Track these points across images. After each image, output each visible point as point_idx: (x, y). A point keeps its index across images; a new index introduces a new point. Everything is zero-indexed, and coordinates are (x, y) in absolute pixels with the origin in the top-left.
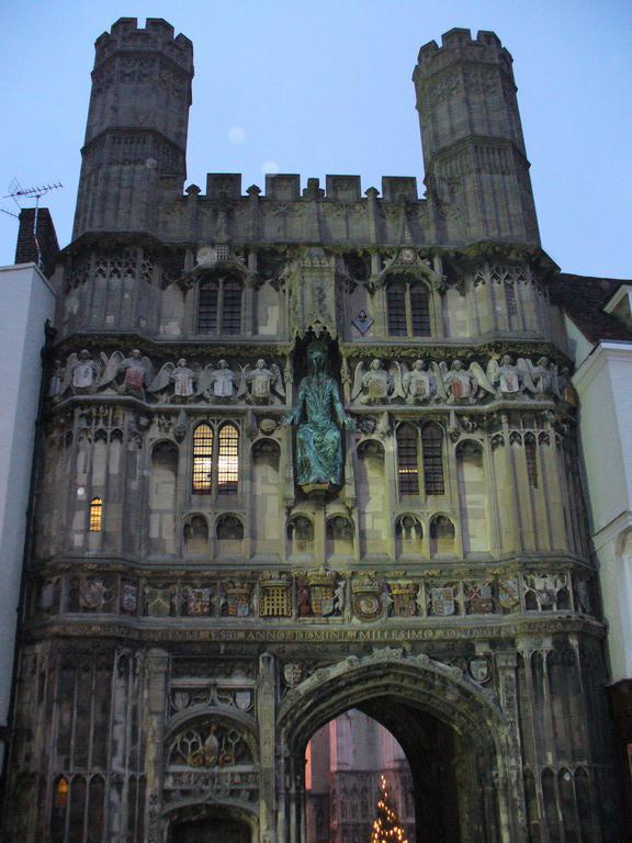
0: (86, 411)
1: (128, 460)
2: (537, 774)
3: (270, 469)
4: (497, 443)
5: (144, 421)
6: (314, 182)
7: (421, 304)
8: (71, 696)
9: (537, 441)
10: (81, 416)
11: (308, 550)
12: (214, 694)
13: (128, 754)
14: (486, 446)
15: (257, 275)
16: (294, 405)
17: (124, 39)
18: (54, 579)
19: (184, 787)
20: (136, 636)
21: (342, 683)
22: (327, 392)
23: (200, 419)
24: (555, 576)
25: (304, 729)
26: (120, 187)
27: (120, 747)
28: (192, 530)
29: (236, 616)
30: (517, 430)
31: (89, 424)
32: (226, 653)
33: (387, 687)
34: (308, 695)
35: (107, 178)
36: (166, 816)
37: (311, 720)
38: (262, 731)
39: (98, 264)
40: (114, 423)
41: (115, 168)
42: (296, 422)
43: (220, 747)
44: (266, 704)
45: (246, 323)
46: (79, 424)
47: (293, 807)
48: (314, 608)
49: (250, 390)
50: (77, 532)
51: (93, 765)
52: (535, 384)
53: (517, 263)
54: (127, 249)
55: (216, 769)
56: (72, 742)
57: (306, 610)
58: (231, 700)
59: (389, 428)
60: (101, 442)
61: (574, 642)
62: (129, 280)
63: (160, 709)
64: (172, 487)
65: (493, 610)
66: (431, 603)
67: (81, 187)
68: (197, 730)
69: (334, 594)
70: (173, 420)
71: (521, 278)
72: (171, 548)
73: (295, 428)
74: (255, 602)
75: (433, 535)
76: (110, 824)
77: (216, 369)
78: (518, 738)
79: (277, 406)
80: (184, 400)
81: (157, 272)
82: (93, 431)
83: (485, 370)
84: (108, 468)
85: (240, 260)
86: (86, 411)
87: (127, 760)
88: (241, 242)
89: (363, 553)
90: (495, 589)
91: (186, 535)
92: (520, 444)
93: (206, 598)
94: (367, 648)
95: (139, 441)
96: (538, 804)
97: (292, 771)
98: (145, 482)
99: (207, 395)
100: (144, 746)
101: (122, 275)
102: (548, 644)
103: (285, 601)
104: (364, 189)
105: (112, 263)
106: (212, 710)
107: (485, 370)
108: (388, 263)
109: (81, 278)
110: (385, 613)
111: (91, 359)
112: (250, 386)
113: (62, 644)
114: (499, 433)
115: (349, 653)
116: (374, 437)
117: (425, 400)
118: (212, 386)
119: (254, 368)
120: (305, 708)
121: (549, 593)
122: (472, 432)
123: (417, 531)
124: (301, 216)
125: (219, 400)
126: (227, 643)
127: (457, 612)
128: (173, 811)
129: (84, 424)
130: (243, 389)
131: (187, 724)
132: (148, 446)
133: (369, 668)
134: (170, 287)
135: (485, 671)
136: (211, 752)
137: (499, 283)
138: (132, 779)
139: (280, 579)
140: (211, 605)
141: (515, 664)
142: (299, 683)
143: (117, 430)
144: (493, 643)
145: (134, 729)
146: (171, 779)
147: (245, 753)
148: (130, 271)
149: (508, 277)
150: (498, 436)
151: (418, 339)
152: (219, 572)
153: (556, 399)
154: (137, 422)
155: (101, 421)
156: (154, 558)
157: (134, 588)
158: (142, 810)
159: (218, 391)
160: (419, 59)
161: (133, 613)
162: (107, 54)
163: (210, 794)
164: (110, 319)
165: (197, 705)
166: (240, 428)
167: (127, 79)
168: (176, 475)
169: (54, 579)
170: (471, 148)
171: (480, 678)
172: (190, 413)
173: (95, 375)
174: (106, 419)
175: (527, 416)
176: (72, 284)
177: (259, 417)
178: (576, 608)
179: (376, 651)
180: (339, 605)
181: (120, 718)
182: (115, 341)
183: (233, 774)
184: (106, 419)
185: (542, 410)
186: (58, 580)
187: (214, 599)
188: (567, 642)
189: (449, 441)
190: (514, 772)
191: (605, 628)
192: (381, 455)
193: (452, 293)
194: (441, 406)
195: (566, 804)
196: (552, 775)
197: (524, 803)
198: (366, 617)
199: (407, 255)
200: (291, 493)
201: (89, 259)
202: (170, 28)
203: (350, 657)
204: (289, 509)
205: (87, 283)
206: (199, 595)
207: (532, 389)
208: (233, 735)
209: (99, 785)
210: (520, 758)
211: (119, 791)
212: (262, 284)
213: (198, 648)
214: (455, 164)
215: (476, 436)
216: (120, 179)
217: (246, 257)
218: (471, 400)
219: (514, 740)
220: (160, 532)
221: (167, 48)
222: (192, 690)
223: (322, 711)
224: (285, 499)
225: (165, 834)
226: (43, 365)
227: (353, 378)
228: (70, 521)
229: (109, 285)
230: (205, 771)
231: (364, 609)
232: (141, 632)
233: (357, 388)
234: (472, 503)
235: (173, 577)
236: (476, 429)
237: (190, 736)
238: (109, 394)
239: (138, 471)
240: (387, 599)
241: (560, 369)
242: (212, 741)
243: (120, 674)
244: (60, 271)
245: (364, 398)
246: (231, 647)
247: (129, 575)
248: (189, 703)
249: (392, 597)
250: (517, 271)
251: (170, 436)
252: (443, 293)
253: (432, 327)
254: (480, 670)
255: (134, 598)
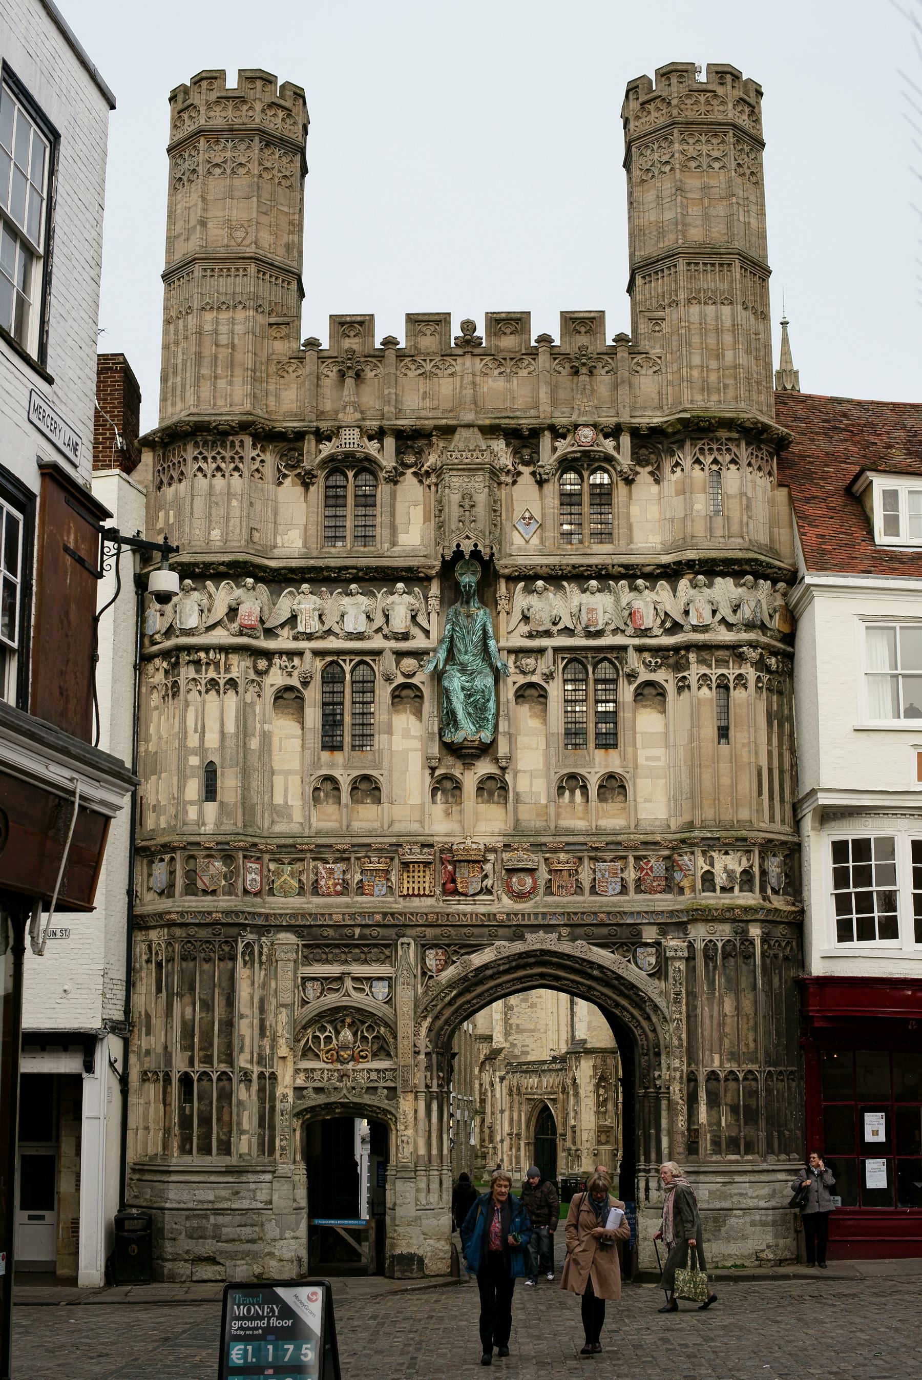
0: (194, 657)
1: (244, 713)
2: (702, 1078)
3: (412, 718)
4: (683, 686)
5: (262, 664)
6: (469, 326)
7: (603, 496)
8: (192, 989)
9: (731, 685)
10: (189, 662)
11: (456, 816)
12: (349, 983)
13: (256, 1049)
14: (671, 688)
15: (395, 468)
16: (441, 642)
17: (209, 106)
18: (167, 857)
19: (318, 1084)
20: (260, 921)
21: (489, 972)
22: (478, 626)
23: (329, 659)
24: (739, 854)
25: (446, 1022)
26: (217, 345)
27: (247, 1042)
28: (322, 794)
29: (372, 895)
30: (708, 671)
31: (198, 671)
32: (362, 937)
33: (542, 976)
34: (451, 985)
35: (199, 333)
36: (298, 1115)
37: (456, 1011)
38: (400, 1024)
39: (196, 458)
40: (227, 670)
41: (208, 316)
42: (441, 666)
43: (355, 1042)
44: (405, 997)
45: (381, 532)
46: (187, 673)
47: (435, 1106)
48: (459, 886)
49: (387, 622)
50: (191, 803)
51: (220, 1062)
52: (735, 611)
53: (728, 439)
54: (231, 438)
55: (350, 1066)
56: (196, 1040)
57: (451, 889)
58: (367, 989)
59: (552, 668)
60: (213, 692)
61: (755, 931)
62: (236, 481)
63: (288, 1001)
64: (297, 742)
65: (668, 889)
66: (594, 879)
67: (166, 332)
68: (330, 1022)
69: (482, 869)
70: (296, 661)
71: (733, 461)
72: (297, 816)
73: (438, 676)
74: (393, 879)
75: (602, 797)
76: (239, 1123)
77: (348, 595)
78: (684, 1036)
79: (419, 642)
80: (310, 637)
81: (269, 470)
82: (203, 682)
83: (674, 590)
84: (222, 725)
85: (372, 448)
86: (194, 657)
87: (255, 1055)
88: (373, 424)
89: (517, 821)
90: (671, 864)
91: (316, 800)
92: (710, 688)
93: (338, 875)
94: (517, 932)
95: (257, 689)
96: (703, 1109)
97: (435, 1068)
98: (266, 737)
99: (336, 629)
100: (274, 1040)
101: (227, 475)
102: (724, 931)
103: (427, 878)
104: (534, 336)
105: (214, 458)
106: (346, 1001)
107: (674, 590)
108: (563, 446)
109: (175, 475)
110: (541, 890)
111: (195, 589)
112: (387, 617)
113: (178, 932)
114: (685, 674)
115: (496, 937)
116: (535, 679)
117: (598, 631)
118: (343, 616)
119: (392, 594)
120: (448, 998)
121: (730, 874)
122: (655, 671)
123: (582, 794)
124: (451, 375)
125: (350, 636)
126: (360, 925)
127: (624, 890)
128: (305, 1109)
129: (192, 674)
130: (379, 621)
131: (320, 1016)
132: (269, 694)
133: (521, 955)
134: (288, 482)
135: (653, 960)
136: (345, 1047)
137: (702, 469)
138: (261, 1076)
139: (421, 854)
140: (345, 883)
141: (686, 955)
142: (441, 970)
143: (231, 679)
144: (664, 928)
145: (262, 1022)
146: (302, 1075)
147: (383, 1050)
148: (236, 469)
149: (715, 461)
150: (684, 677)
151: (597, 548)
152: (353, 846)
153: (763, 627)
154: (255, 667)
155: (212, 667)
156: (279, 828)
157: (258, 866)
158: (273, 1109)
159: (350, 627)
160: (627, 96)
161: (257, 894)
162: (189, 127)
163: (345, 1091)
164: (216, 534)
165: (329, 996)
166: (376, 668)
167: (218, 171)
168: (303, 729)
169: (167, 857)
170: (681, 265)
171: (646, 967)
172: (317, 653)
173: (202, 611)
174: (217, 665)
175: (720, 653)
176: (165, 481)
177: (400, 655)
178: (763, 890)
179: (528, 936)
180: (489, 882)
181: (245, 1010)
182: (222, 568)
183: (370, 1070)
184: (217, 665)
185: (741, 646)
186: (172, 859)
187: (349, 877)
188: (745, 932)
189: (626, 682)
190: (678, 1074)
191: (802, 912)
192: (542, 700)
193: (644, 473)
194: (619, 640)
195: (734, 1109)
196: (717, 1079)
197: (685, 1108)
198: (520, 896)
199: (586, 435)
200: (435, 750)
201: (185, 450)
202: (268, 79)
203: (497, 943)
204: (433, 769)
205: (183, 484)
206: (331, 872)
207: (731, 619)
208: (370, 1028)
209: (226, 1083)
210: (685, 1059)
211: (248, 1089)
212: (403, 474)
213: (331, 932)
214: (659, 286)
215: (660, 676)
216: (216, 332)
217: (381, 441)
218: (657, 631)
219: (680, 1039)
220: (286, 796)
221: (270, 113)
222: (326, 979)
223: (469, 1002)
224: (429, 759)
225: (298, 1133)
226: (137, 593)
227: (510, 599)
228: (182, 787)
229: (211, 486)
230: (339, 1067)
231: (516, 887)
232: (267, 916)
233: (517, 616)
234: (648, 759)
235: (302, 851)
236: (660, 666)
237: (323, 1029)
238: (220, 636)
239: (258, 726)
240: (543, 875)
241: (774, 582)
242: (347, 1035)
243: (245, 963)
244: (147, 458)
245: (524, 629)
246: (367, 931)
247: (252, 852)
248: (321, 993)
249: (550, 872)
250: (728, 450)
251: (295, 682)
252: (629, 482)
253: (615, 532)
254: (649, 958)
255: (258, 878)
